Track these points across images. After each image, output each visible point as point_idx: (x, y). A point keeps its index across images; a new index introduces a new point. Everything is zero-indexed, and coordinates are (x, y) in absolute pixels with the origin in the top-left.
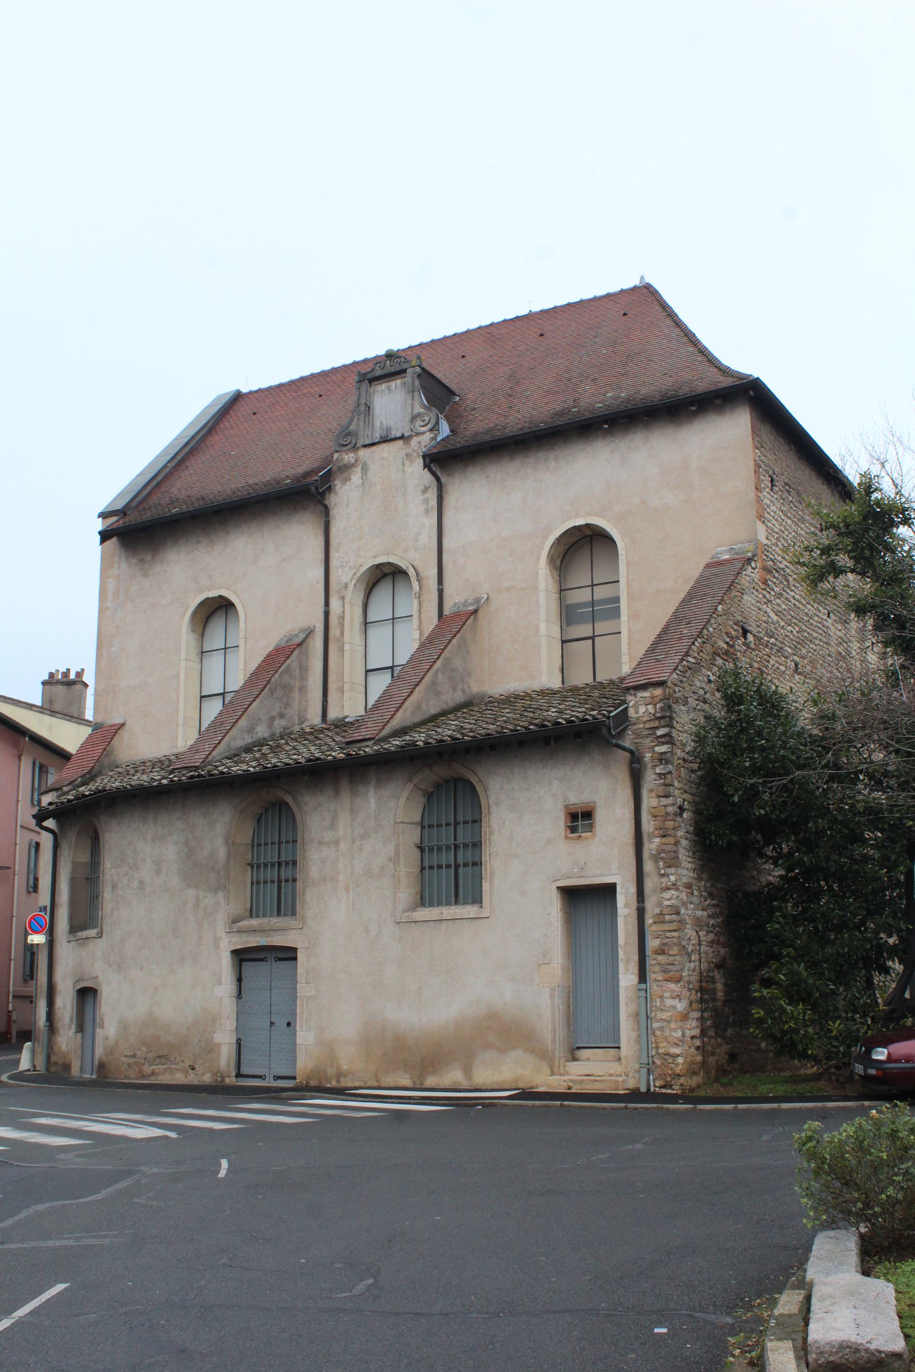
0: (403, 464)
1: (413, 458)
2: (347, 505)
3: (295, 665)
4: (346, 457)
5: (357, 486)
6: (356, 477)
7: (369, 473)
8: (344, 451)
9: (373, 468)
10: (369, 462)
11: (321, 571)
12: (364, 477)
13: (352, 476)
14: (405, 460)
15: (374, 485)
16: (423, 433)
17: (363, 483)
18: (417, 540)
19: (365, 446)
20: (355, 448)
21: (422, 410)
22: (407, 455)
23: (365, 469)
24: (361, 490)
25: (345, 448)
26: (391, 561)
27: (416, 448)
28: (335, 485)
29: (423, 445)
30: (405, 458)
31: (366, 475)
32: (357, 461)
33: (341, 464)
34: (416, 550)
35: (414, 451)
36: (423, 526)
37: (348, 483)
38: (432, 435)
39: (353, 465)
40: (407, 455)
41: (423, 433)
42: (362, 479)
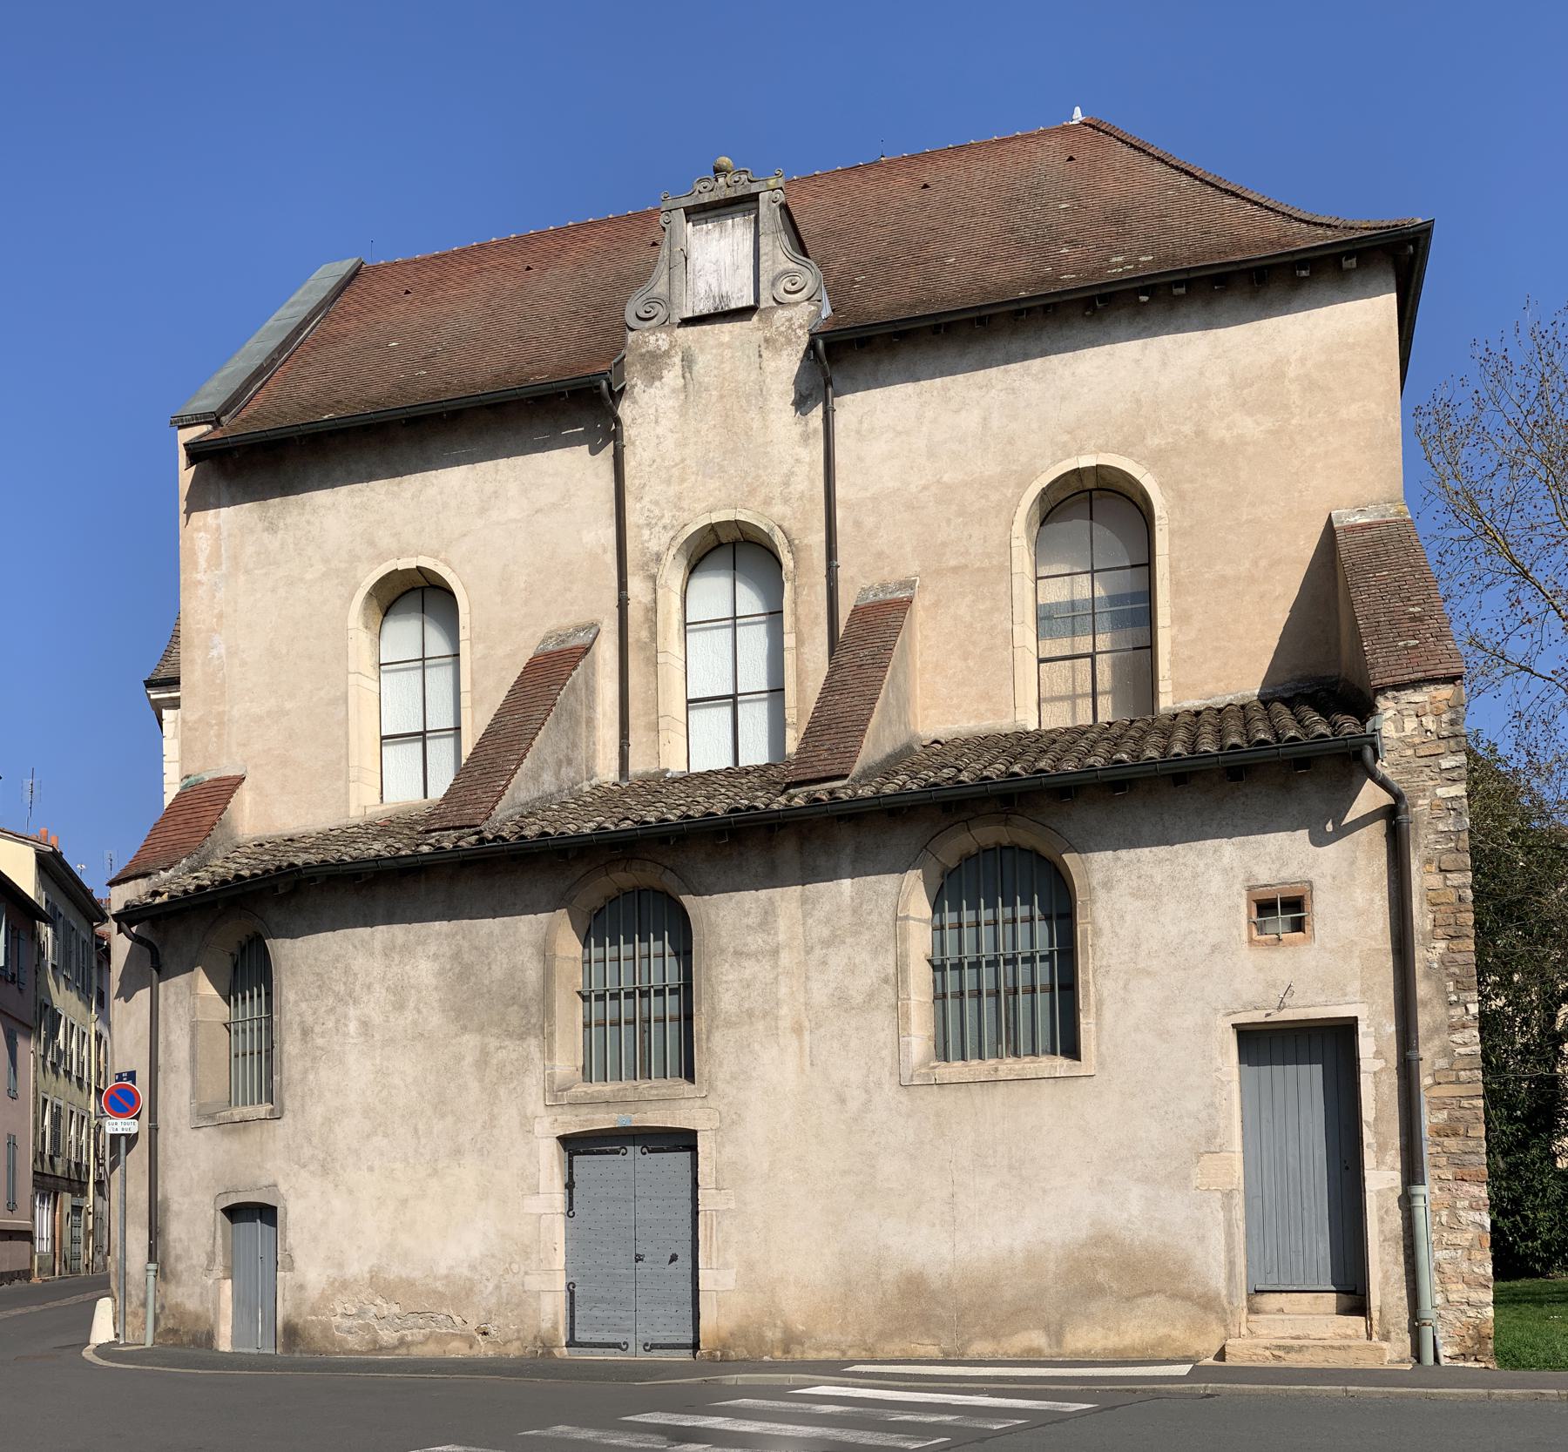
0: (760, 356)
1: (778, 345)
2: (656, 422)
3: (581, 680)
4: (652, 339)
5: (674, 391)
6: (672, 376)
7: (695, 368)
8: (648, 330)
9: (702, 361)
10: (695, 350)
11: (612, 532)
12: (688, 375)
13: (665, 372)
14: (762, 349)
15: (707, 390)
16: (797, 303)
17: (685, 386)
18: (787, 484)
19: (687, 322)
20: (665, 325)
21: (792, 265)
22: (767, 340)
23: (688, 362)
24: (682, 397)
25: (647, 324)
26: (741, 518)
27: (783, 329)
28: (633, 387)
29: (797, 324)
30: (763, 346)
31: (691, 373)
32: (672, 346)
33: (644, 350)
34: (786, 501)
35: (781, 333)
36: (797, 460)
37: (657, 383)
38: (813, 308)
39: (667, 354)
40: (767, 340)
41: (797, 303)
42: (684, 377)
